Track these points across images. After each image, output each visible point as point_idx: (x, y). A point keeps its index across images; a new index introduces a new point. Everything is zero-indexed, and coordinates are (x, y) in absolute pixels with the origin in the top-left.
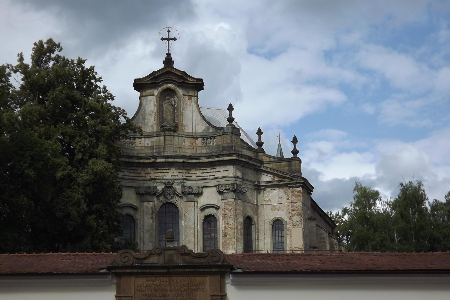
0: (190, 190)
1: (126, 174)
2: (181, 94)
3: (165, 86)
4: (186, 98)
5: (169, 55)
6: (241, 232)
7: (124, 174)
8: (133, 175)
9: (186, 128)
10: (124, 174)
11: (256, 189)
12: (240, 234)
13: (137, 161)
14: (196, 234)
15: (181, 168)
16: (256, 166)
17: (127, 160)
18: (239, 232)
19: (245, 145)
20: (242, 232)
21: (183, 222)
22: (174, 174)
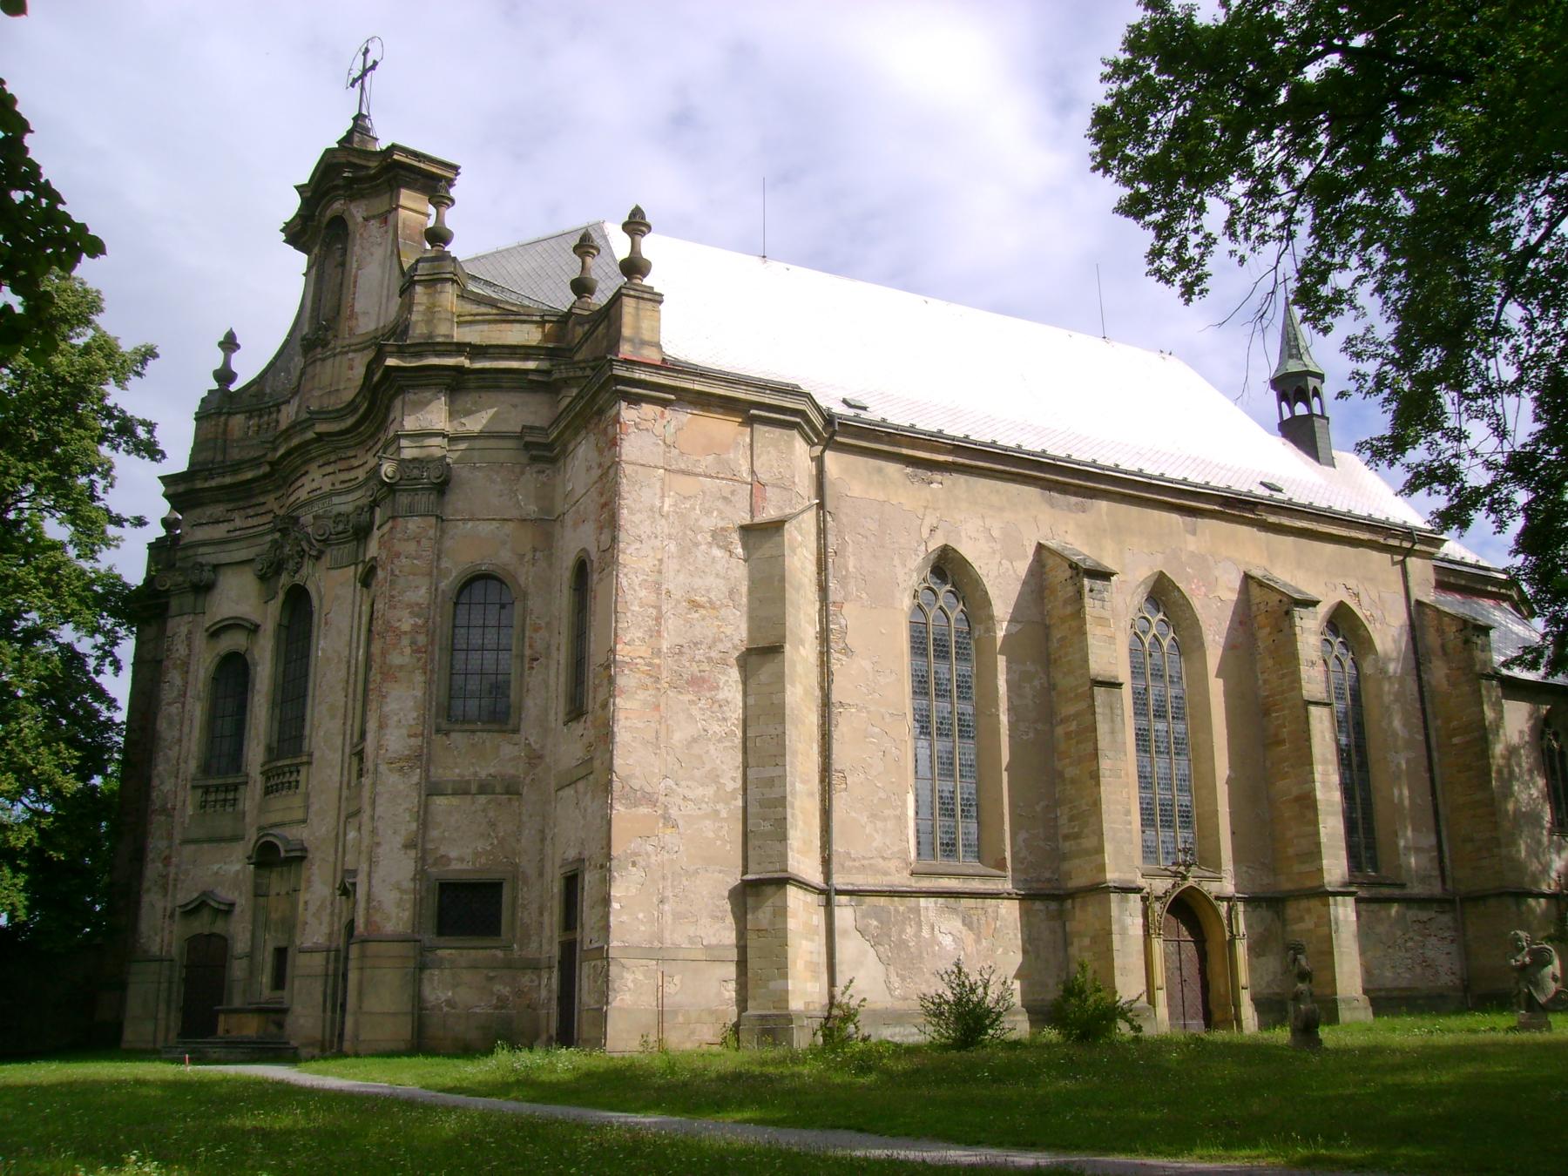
0: (341, 528)
1: (238, 523)
2: (360, 219)
3: (329, 214)
4: (374, 224)
5: (359, 118)
6: (413, 643)
7: (230, 526)
8: (254, 521)
9: (362, 321)
10: (230, 526)
11: (534, 459)
12: (408, 651)
13: (249, 475)
14: (352, 681)
15: (333, 458)
16: (526, 372)
17: (228, 480)
18: (405, 641)
19: (483, 309)
20: (422, 639)
21: (322, 643)
22: (315, 485)
